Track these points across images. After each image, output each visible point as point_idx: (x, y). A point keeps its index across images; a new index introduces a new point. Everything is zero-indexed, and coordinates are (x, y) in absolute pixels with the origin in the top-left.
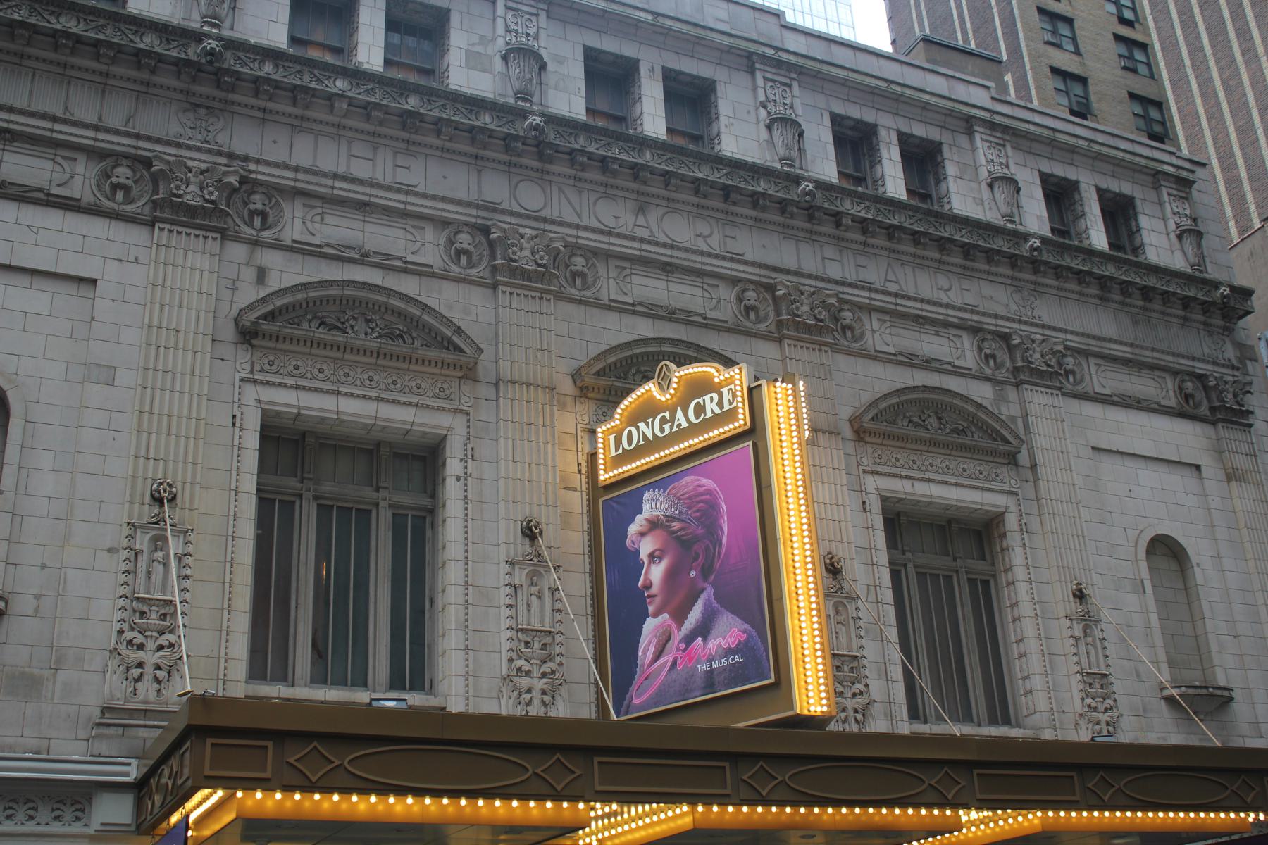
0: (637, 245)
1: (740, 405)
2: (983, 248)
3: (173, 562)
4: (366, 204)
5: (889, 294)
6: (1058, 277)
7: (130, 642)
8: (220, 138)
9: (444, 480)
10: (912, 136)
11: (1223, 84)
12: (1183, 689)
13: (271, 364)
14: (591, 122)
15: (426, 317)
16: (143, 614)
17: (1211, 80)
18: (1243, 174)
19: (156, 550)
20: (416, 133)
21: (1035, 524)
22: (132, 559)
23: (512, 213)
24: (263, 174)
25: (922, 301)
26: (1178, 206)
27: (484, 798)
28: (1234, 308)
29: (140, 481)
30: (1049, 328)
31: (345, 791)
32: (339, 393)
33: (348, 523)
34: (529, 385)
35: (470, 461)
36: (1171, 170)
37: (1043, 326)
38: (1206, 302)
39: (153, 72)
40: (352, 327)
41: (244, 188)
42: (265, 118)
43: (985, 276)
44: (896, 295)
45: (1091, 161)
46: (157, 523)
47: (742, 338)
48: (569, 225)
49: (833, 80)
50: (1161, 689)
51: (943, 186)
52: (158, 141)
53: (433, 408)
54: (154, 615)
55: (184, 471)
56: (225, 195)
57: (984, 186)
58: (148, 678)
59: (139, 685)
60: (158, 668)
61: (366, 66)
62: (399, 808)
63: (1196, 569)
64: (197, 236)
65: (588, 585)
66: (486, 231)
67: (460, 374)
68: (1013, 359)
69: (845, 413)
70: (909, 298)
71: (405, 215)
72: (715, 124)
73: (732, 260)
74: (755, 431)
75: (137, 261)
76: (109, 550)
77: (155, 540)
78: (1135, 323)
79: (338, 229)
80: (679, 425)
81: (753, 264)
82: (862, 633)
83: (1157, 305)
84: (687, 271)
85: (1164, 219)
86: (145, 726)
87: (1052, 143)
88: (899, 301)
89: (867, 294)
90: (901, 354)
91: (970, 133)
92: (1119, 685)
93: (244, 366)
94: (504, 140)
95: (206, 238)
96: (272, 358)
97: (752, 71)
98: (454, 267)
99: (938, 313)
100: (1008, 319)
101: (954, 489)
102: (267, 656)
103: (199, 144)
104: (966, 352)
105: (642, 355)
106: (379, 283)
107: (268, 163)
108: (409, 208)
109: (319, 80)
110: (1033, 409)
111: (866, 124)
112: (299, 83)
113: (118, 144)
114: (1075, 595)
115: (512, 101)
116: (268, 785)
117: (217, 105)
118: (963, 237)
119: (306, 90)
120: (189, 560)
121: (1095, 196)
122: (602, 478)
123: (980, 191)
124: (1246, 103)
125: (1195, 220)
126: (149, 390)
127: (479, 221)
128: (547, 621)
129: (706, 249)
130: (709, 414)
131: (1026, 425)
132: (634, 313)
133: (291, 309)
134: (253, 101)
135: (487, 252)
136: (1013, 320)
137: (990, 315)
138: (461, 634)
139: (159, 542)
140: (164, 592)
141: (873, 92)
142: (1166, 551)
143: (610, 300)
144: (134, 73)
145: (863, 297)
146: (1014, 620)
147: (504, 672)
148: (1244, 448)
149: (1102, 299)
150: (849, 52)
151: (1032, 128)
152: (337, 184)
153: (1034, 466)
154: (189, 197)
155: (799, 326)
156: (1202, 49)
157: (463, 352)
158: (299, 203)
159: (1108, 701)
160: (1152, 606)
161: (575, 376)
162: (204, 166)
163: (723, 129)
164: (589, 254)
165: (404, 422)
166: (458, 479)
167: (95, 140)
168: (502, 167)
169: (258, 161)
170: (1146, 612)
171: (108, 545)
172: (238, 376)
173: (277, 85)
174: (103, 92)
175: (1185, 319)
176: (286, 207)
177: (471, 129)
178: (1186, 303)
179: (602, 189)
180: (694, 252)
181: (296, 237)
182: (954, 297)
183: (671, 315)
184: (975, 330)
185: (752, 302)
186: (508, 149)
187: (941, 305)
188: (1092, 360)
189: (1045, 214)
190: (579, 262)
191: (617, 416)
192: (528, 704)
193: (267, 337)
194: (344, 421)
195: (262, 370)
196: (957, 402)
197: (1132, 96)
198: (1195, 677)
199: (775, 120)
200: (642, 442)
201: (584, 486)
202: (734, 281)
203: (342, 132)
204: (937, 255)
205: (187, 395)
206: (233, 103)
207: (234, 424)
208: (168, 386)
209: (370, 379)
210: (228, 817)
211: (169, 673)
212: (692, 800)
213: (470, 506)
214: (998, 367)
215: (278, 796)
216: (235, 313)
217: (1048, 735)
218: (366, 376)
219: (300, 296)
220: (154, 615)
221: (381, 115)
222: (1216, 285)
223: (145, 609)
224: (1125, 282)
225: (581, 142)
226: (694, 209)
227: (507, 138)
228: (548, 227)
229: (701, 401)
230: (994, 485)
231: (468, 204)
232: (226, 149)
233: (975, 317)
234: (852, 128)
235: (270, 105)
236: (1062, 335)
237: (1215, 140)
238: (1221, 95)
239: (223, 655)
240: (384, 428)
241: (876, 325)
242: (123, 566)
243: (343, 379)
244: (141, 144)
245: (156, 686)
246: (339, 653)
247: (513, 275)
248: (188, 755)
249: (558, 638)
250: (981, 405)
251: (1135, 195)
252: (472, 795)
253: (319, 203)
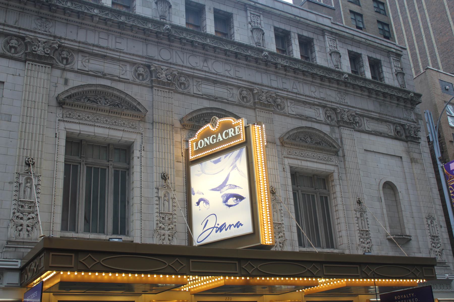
0: (204, 73)
1: (242, 133)
2: (328, 77)
3: (34, 187)
4: (105, 56)
5: (294, 93)
6: (354, 88)
7: (18, 217)
8: (51, 30)
9: (133, 158)
10: (303, 36)
11: (411, 19)
12: (394, 236)
13: (70, 114)
14: (187, 28)
15: (127, 98)
16: (22, 206)
17: (407, 17)
18: (418, 52)
19: (27, 183)
20: (124, 30)
21: (344, 177)
22: (18, 186)
23: (158, 61)
24: (67, 44)
25: (306, 96)
26: (396, 64)
27: (150, 274)
28: (415, 101)
29: (21, 157)
30: (350, 106)
31: (100, 272)
32: (95, 126)
33: (97, 174)
34: (164, 124)
35: (143, 151)
36: (394, 51)
37: (348, 106)
38: (405, 98)
39: (25, 4)
40: (100, 101)
41: (60, 49)
42: (67, 23)
43: (328, 87)
44: (296, 94)
46: (27, 173)
47: (241, 108)
48: (179, 65)
49: (275, 15)
50: (387, 236)
51: (314, 54)
52: (27, 30)
53: (129, 131)
54: (26, 207)
55: (38, 153)
56: (53, 51)
57: (328, 55)
58: (24, 230)
59: (21, 232)
60: (28, 226)
61: (105, 5)
62: (119, 278)
63: (400, 194)
64: (42, 66)
65: (185, 197)
66: (149, 67)
67: (139, 119)
68: (337, 118)
69: (278, 136)
70: (301, 95)
71: (119, 60)
72: (232, 29)
73: (238, 79)
74: (247, 143)
75: (19, 75)
76: (9, 183)
77: (27, 179)
78: (381, 105)
79: (95, 65)
80: (219, 140)
81: (245, 81)
82: (283, 215)
83: (388, 99)
84: (222, 83)
85: (391, 68)
86: (23, 248)
87: (352, 40)
88: (297, 96)
89: (286, 93)
90: (298, 115)
91: (323, 35)
92: (372, 234)
93: (60, 115)
94: (156, 33)
95: (45, 67)
96: (70, 112)
97: (246, 11)
98: (137, 80)
99: (311, 100)
100: (336, 103)
101: (315, 164)
102: (68, 222)
103: (43, 32)
104: (320, 114)
105: (205, 113)
106: (109, 85)
107: (69, 40)
108: (121, 58)
109: (88, 9)
110: (344, 136)
111: (287, 31)
112: (80, 10)
113: (12, 31)
114: (357, 202)
115: (159, 19)
116: (72, 270)
117: (49, 17)
118: (320, 73)
119: (83, 13)
120: (40, 187)
121: (367, 59)
122: (190, 158)
123: (327, 57)
124: (419, 26)
125: (402, 69)
126: (24, 124)
127: (147, 63)
128: (171, 210)
129: (229, 75)
130: (230, 136)
131: (341, 141)
132: (202, 98)
133: (77, 94)
134: (63, 16)
135: (149, 74)
136: (338, 104)
137: (329, 102)
138: (139, 214)
139: (29, 180)
140: (30, 198)
141: (289, 19)
142: (389, 187)
143: (194, 93)
144: (18, 5)
145: (284, 94)
146: (336, 211)
147: (155, 228)
148: (417, 151)
149: (369, 96)
150: (281, 4)
151: (346, 34)
152: (95, 48)
153: (344, 156)
154: (39, 52)
155: (261, 104)
156: (404, 6)
157: (141, 111)
158: (80, 55)
159: (368, 240)
160: (384, 206)
161: (181, 121)
162: (45, 40)
163: (235, 31)
164: (186, 76)
165: (118, 137)
166: (138, 158)
167: (3, 29)
168: (155, 43)
169: (65, 39)
170: (382, 209)
171: (9, 181)
172: (57, 119)
173: (72, 11)
174: (6, 11)
175: (398, 104)
176: (75, 56)
177: (144, 29)
178: (398, 98)
179: (191, 52)
180: (224, 76)
181: (79, 68)
182: (317, 95)
183: (216, 99)
184: (324, 107)
185: (245, 95)
186: (157, 37)
187: (312, 97)
188: (365, 119)
189: (349, 65)
190: (183, 79)
191: (196, 136)
192: (164, 240)
193: (68, 104)
194: (96, 136)
195: (67, 117)
196: (317, 132)
197: (379, 22)
198: (398, 232)
199: (254, 29)
200: (205, 146)
201: (184, 161)
202: (239, 87)
203: (96, 29)
204: (311, 79)
205: (38, 126)
206: (55, 17)
207: (56, 137)
208: (32, 122)
209: (106, 121)
210: (57, 281)
211: (32, 228)
212: (224, 275)
213: (142, 168)
214: (332, 120)
215: (76, 273)
216: (56, 95)
217: (347, 252)
218: (105, 120)
219: (81, 90)
220: (26, 207)
221: (111, 23)
222: (409, 92)
223: (23, 204)
224: (377, 90)
225: (184, 35)
226: (225, 61)
227: (157, 33)
228: (172, 66)
229: (227, 131)
230: (330, 163)
231: (142, 57)
232: (53, 34)
233: (324, 102)
234: (282, 32)
235: (69, 18)
236: (355, 109)
237: (408, 39)
238: (411, 23)
239: (52, 221)
240: (111, 139)
241: (289, 104)
242: (15, 189)
243: (96, 121)
244: (21, 31)
245: (27, 233)
246: (94, 221)
247: (159, 84)
248: (43, 258)
249: (175, 216)
250: (326, 134)
251: (381, 59)
252: (146, 273)
253: (87, 55)
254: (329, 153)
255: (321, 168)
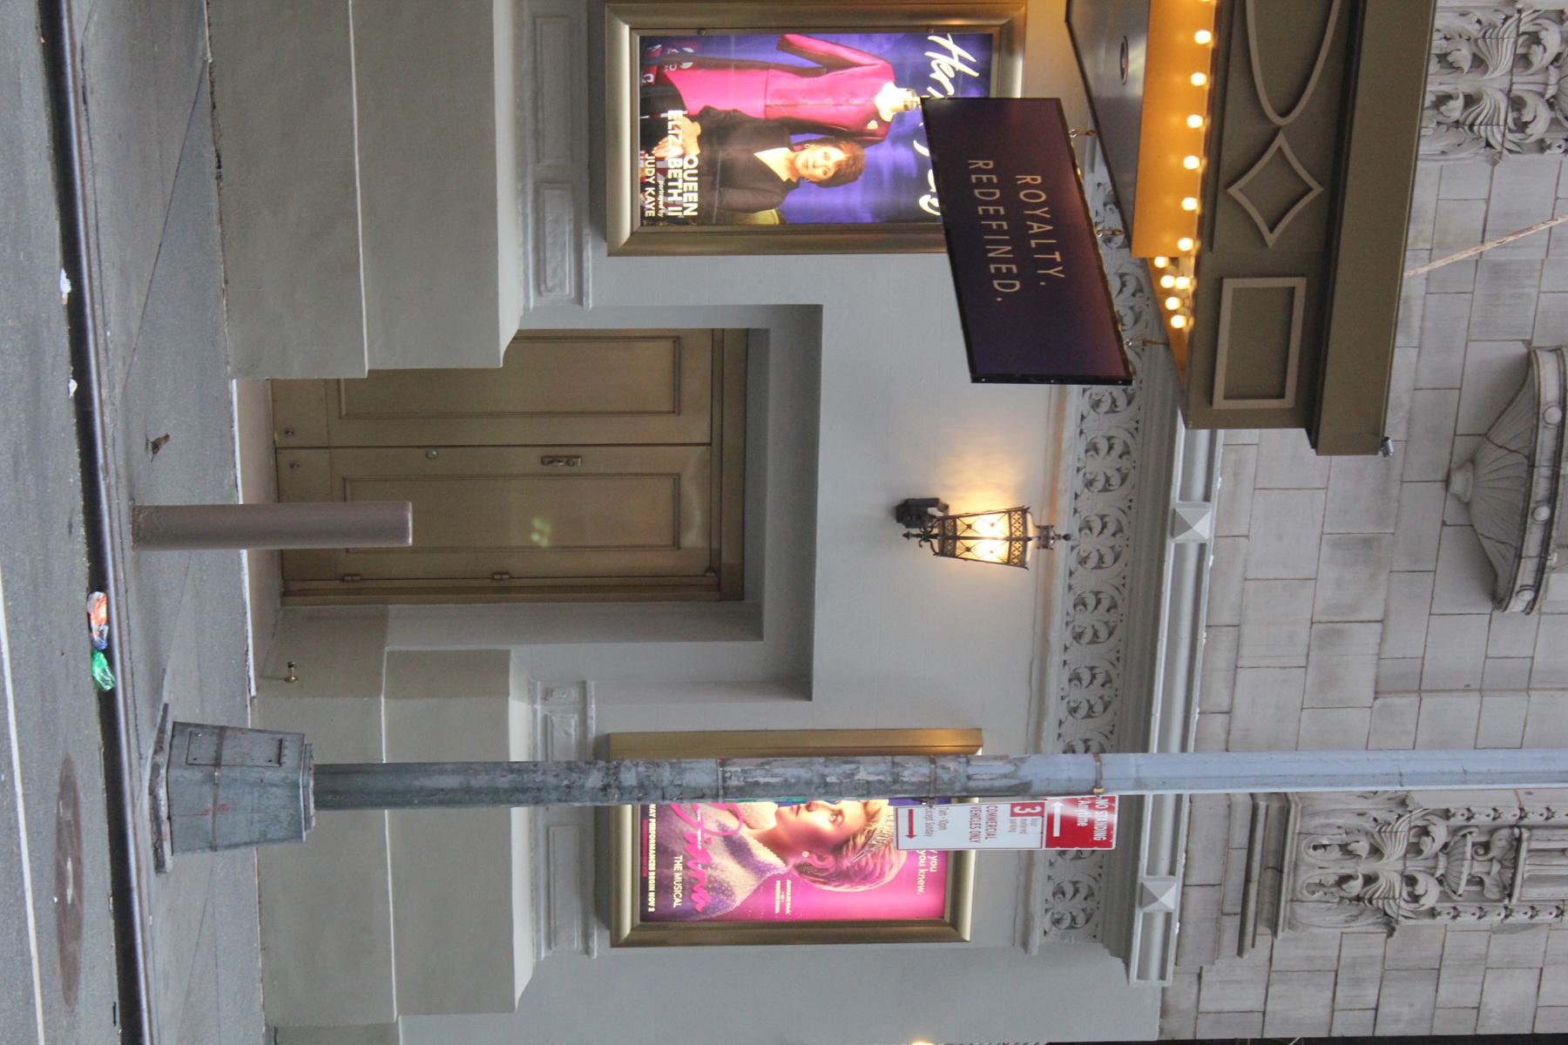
7: (1425, 831)
59: (1336, 853)
211: (1358, 898)
220: (1479, 869)
245: (1332, 879)
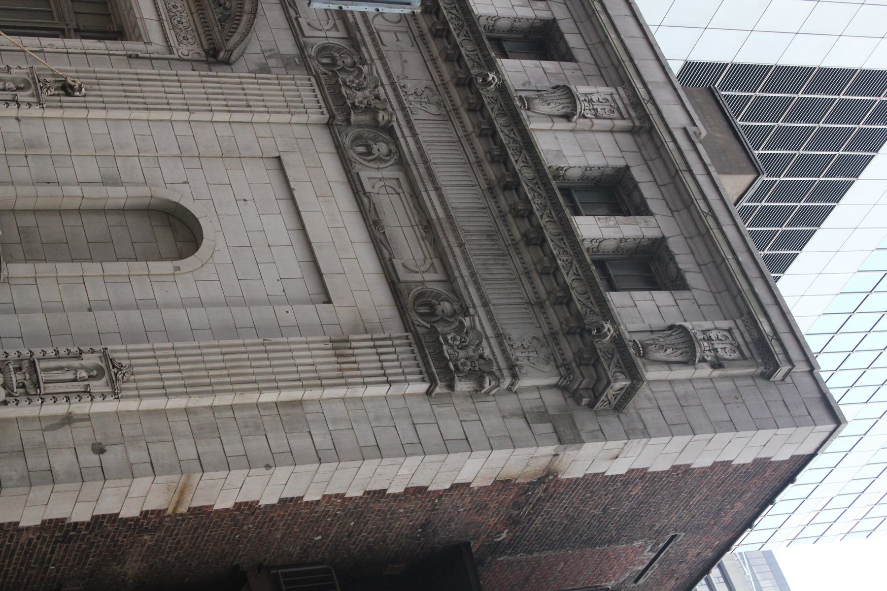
10: (561, 35)
36: (767, 328)
43: (427, 57)
45: (694, 231)
83: (529, 255)
87: (674, 176)
149: (491, 189)
151: (671, 145)
230: (171, 34)
254: (201, 31)
255: (142, 6)
